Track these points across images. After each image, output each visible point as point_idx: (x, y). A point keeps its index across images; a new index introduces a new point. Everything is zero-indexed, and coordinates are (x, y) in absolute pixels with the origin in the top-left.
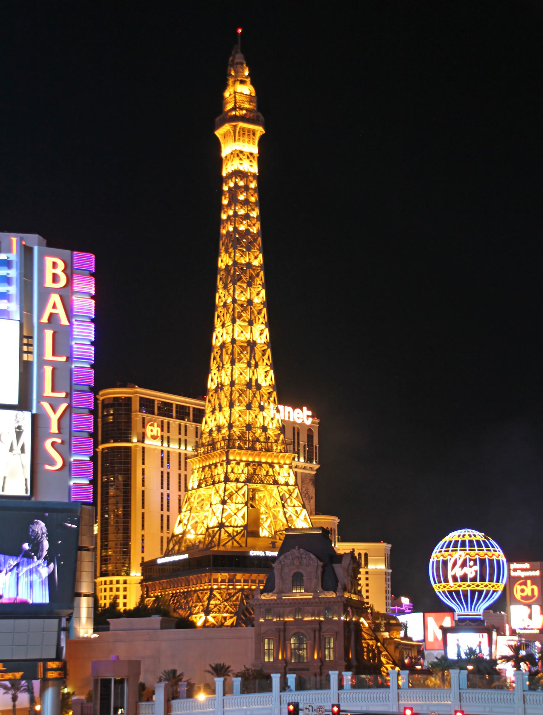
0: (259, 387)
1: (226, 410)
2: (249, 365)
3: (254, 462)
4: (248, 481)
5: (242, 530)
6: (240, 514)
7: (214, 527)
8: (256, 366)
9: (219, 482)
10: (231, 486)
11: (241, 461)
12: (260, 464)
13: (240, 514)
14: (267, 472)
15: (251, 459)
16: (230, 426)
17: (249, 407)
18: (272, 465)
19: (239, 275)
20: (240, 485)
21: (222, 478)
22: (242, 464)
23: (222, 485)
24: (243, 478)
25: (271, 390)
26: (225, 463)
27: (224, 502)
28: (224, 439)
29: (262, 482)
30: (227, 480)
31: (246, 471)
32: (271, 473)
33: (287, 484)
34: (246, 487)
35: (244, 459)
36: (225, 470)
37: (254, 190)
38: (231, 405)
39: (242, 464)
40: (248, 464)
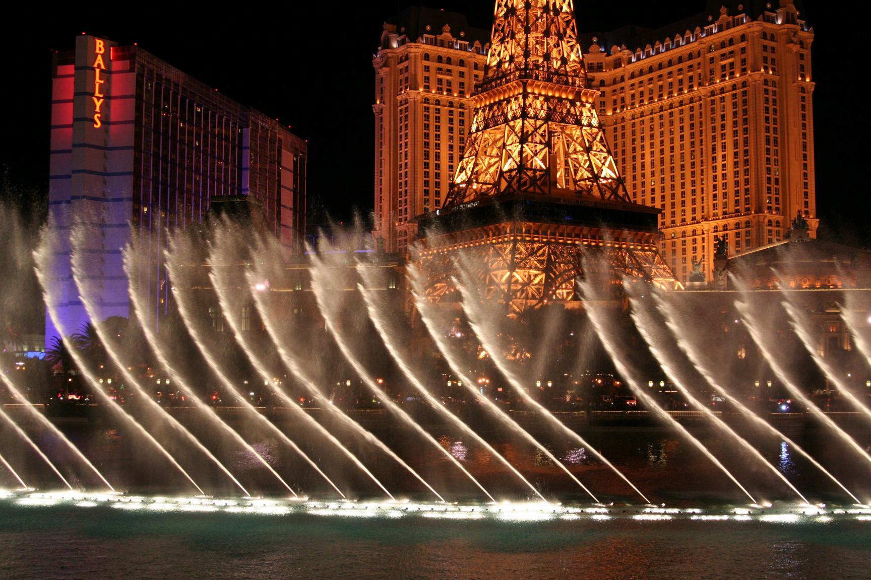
0: (557, 12)
1: (521, 36)
3: (553, 97)
4: (547, 119)
5: (541, 176)
6: (541, 156)
7: (510, 171)
9: (514, 118)
10: (529, 124)
11: (540, 94)
12: (560, 99)
13: (541, 156)
14: (569, 111)
15: (550, 94)
16: (527, 54)
17: (547, 34)
18: (573, 103)
20: (539, 123)
21: (519, 113)
22: (541, 99)
23: (519, 123)
24: (542, 114)
25: (570, 18)
26: (520, 97)
27: (523, 140)
28: (517, 68)
29: (563, 120)
30: (524, 116)
31: (545, 106)
32: (572, 110)
33: (590, 125)
34: (546, 125)
35: (543, 93)
36: (522, 104)
38: (527, 31)
39: (541, 99)
40: (547, 99)
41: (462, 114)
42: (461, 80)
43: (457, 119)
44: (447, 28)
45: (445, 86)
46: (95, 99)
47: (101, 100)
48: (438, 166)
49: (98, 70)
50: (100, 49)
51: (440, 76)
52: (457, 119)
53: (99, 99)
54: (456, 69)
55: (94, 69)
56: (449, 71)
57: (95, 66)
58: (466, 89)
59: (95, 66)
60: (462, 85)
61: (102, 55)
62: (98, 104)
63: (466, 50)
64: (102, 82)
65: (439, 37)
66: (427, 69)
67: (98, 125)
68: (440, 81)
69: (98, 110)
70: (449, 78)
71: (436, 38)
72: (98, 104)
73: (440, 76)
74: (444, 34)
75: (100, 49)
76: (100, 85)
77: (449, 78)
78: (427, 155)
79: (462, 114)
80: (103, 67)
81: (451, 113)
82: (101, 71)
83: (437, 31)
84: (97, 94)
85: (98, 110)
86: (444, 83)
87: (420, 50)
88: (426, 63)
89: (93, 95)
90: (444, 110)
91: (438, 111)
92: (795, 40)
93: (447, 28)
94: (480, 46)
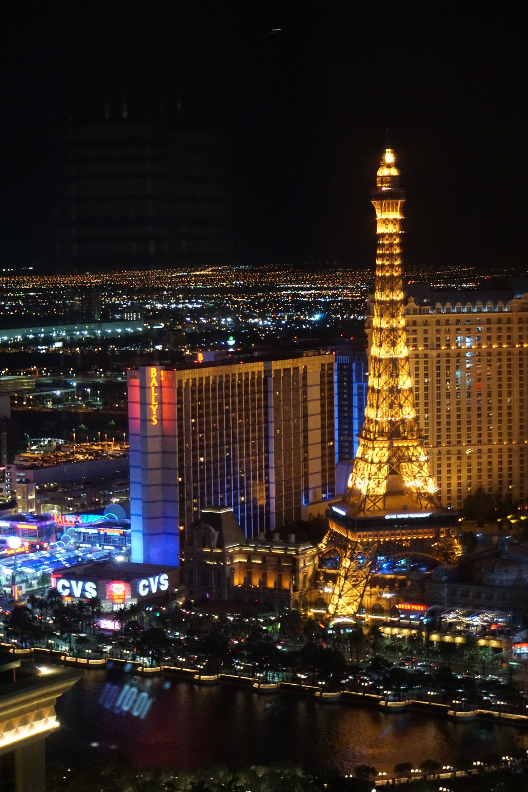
37: (397, 245)
41: (426, 362)
42: (426, 336)
46: (152, 407)
47: (157, 406)
49: (153, 388)
50: (154, 374)
53: (155, 406)
55: (150, 388)
57: (151, 385)
59: (151, 385)
61: (155, 377)
62: (154, 409)
63: (428, 313)
64: (156, 394)
67: (155, 422)
69: (154, 413)
70: (415, 336)
72: (154, 409)
75: (154, 374)
76: (155, 397)
77: (415, 336)
80: (156, 385)
82: (156, 387)
84: (154, 403)
85: (154, 413)
89: (151, 405)
94: (441, 307)
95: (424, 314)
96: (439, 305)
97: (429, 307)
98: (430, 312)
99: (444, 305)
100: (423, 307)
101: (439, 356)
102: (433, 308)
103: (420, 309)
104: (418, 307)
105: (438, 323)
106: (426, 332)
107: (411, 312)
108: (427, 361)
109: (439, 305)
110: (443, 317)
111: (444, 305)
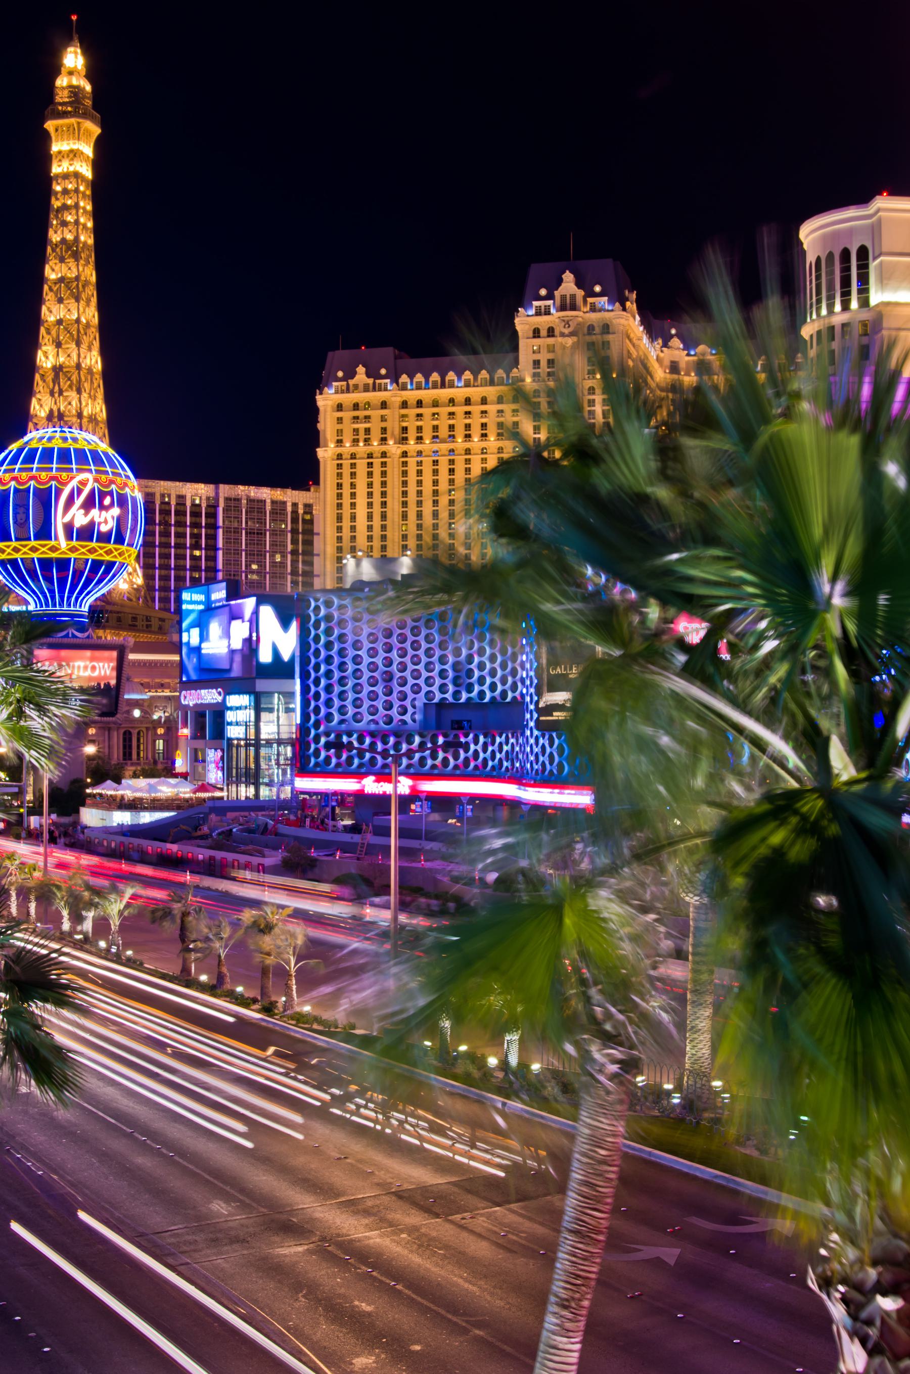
2: (52, 394)
8: (61, 393)
19: (71, 288)
41: (384, 464)
42: (384, 425)
43: (377, 470)
44: (361, 370)
45: (362, 436)
48: (353, 529)
51: (356, 426)
52: (377, 470)
54: (376, 414)
56: (367, 418)
58: (388, 435)
60: (384, 430)
63: (386, 390)
65: (351, 382)
66: (340, 420)
68: (356, 431)
70: (367, 425)
71: (348, 385)
73: (356, 426)
74: (357, 377)
77: (367, 425)
78: (339, 518)
79: (384, 464)
81: (370, 465)
83: (350, 374)
86: (362, 432)
87: (330, 403)
88: (340, 414)
90: (362, 465)
91: (353, 466)
92: (566, 331)
93: (361, 370)
95: (380, 390)
96: (404, 378)
97: (388, 381)
98: (389, 387)
99: (411, 377)
100: (378, 381)
101: (405, 454)
102: (395, 380)
103: (374, 383)
104: (370, 381)
105: (404, 405)
106: (383, 419)
107: (361, 387)
108: (385, 463)
109: (404, 378)
110: (412, 395)
111: (411, 377)
